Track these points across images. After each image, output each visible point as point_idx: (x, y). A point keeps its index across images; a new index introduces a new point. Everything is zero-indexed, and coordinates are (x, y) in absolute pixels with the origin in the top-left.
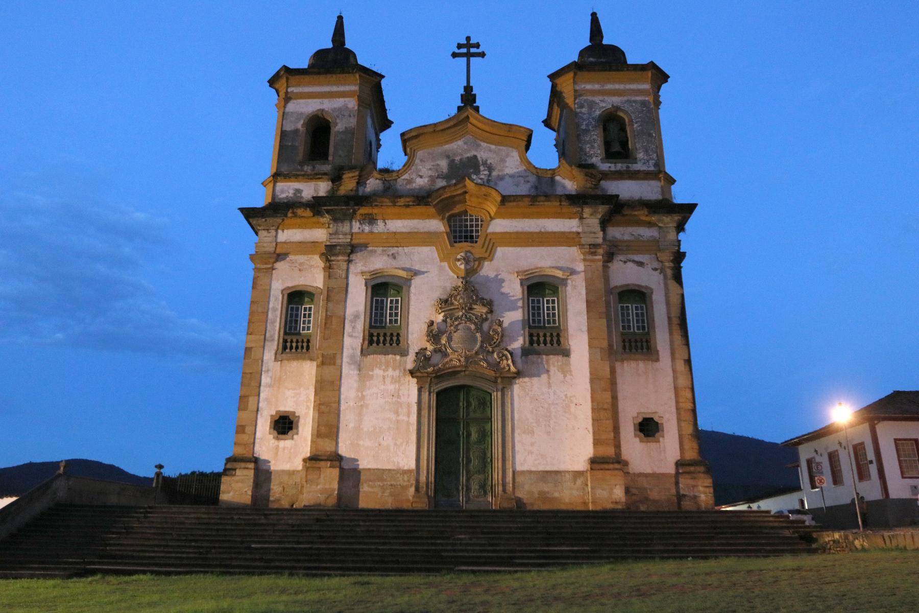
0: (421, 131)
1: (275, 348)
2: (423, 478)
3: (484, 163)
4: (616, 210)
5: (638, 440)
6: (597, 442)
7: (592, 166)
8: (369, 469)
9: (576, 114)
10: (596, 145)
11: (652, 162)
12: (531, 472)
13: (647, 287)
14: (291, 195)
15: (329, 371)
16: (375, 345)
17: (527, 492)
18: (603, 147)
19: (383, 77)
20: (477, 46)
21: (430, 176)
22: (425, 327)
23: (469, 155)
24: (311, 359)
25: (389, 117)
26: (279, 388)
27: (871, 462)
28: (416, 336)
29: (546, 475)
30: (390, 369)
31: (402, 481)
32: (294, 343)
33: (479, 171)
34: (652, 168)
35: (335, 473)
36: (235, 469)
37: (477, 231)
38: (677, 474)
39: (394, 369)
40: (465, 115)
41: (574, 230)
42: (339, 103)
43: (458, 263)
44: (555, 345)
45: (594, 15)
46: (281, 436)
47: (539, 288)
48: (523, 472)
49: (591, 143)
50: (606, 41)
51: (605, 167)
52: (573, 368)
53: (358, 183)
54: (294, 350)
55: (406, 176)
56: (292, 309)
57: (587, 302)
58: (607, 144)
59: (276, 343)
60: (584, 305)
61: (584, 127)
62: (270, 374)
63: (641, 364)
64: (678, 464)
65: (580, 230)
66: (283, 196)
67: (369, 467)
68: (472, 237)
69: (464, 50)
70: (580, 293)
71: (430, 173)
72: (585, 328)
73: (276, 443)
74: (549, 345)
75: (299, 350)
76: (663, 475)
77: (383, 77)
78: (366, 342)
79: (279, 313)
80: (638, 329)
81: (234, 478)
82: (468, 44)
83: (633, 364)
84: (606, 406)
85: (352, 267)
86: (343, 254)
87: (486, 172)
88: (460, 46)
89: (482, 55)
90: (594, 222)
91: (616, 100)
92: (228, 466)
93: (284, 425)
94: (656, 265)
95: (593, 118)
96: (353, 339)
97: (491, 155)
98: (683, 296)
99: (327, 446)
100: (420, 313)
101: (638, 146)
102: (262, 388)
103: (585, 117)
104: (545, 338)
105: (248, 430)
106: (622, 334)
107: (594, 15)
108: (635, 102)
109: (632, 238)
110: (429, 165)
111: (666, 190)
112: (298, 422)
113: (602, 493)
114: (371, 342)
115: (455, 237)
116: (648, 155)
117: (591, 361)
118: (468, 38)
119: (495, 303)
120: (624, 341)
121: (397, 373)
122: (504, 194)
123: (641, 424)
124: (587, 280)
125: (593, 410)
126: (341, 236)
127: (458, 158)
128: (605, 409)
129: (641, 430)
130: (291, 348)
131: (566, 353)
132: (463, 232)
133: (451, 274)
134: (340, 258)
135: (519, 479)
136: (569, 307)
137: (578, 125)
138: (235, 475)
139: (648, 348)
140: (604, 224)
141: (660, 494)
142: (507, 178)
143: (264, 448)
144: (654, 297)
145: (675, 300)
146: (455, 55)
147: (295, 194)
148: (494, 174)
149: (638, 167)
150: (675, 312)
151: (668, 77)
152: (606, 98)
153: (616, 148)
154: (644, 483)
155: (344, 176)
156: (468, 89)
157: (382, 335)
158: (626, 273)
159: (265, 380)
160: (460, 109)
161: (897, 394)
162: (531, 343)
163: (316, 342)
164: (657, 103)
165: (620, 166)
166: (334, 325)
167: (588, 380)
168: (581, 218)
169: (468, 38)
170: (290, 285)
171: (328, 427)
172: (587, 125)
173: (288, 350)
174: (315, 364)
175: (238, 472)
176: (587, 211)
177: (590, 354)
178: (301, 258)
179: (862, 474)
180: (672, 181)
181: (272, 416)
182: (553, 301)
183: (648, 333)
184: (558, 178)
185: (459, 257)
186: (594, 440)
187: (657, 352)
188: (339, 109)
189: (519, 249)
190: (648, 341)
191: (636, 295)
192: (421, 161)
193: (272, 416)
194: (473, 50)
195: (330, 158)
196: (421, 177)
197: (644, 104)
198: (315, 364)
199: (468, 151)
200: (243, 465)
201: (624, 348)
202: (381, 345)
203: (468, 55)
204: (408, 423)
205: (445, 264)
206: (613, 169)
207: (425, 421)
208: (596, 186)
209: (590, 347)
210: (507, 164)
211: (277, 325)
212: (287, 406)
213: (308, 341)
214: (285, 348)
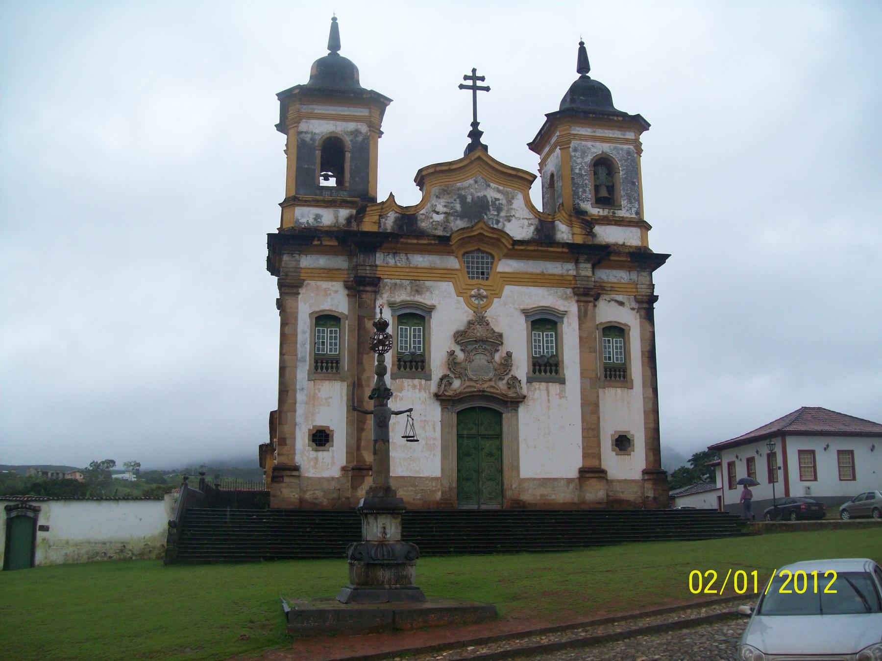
0: (438, 169)
1: (308, 368)
3: (494, 203)
4: (602, 255)
5: (614, 453)
6: (585, 456)
7: (585, 213)
8: (403, 477)
9: (571, 157)
10: (587, 189)
11: (634, 210)
12: (534, 479)
13: (626, 325)
14: (311, 221)
16: (402, 369)
17: (529, 496)
18: (593, 192)
20: (482, 79)
21: (445, 213)
23: (479, 194)
26: (314, 405)
27: (780, 468)
29: (545, 482)
30: (417, 391)
33: (489, 210)
34: (634, 216)
36: (282, 477)
37: (487, 268)
38: (644, 480)
39: (420, 390)
40: (477, 155)
41: (571, 272)
42: (351, 126)
43: (473, 299)
44: (553, 373)
45: (582, 44)
46: (319, 448)
48: (528, 479)
49: (584, 186)
50: (593, 75)
51: (595, 211)
52: (567, 394)
53: (380, 216)
54: (324, 370)
56: (319, 331)
57: (580, 338)
58: (597, 188)
59: (308, 363)
60: (577, 341)
61: (577, 171)
62: (305, 392)
63: (619, 390)
64: (645, 472)
65: (575, 273)
66: (303, 220)
67: (401, 474)
68: (483, 273)
69: (470, 83)
70: (574, 330)
71: (445, 210)
72: (578, 361)
73: (313, 454)
74: (548, 374)
75: (330, 370)
76: (634, 481)
78: (396, 367)
79: (308, 335)
80: (617, 360)
81: (284, 485)
82: (474, 77)
83: (613, 390)
84: (593, 426)
85: (378, 297)
86: (370, 284)
87: (496, 213)
88: (466, 78)
89: (487, 89)
90: (589, 266)
91: (606, 147)
92: (275, 474)
94: (634, 305)
95: (585, 163)
97: (498, 196)
98: (653, 333)
100: (440, 344)
101: (622, 193)
102: (298, 405)
103: (579, 161)
104: (547, 368)
105: (288, 441)
106: (605, 363)
107: (582, 44)
108: (622, 149)
109: (615, 280)
111: (644, 238)
112: (333, 436)
114: (399, 369)
115: (468, 273)
116: (631, 203)
117: (582, 389)
118: (474, 70)
119: (505, 336)
120: (606, 371)
121: (423, 395)
123: (617, 440)
125: (583, 429)
126: (368, 268)
128: (593, 429)
129: (617, 445)
130: (322, 368)
131: (562, 382)
133: (467, 308)
134: (368, 288)
135: (526, 485)
136: (565, 341)
137: (572, 169)
138: (283, 482)
139: (624, 377)
140: (594, 267)
141: (630, 495)
142: (513, 219)
143: (305, 458)
144: (631, 333)
145: (648, 335)
146: (462, 87)
147: (315, 219)
148: (503, 214)
149: (622, 213)
150: (648, 348)
151: (650, 125)
152: (598, 144)
153: (604, 193)
155: (368, 209)
156: (475, 124)
158: (608, 312)
159: (301, 397)
160: (470, 149)
161: (804, 410)
162: (534, 372)
163: (345, 363)
164: (639, 151)
167: (579, 405)
169: (474, 70)
170: (317, 309)
172: (580, 169)
173: (319, 370)
174: (345, 384)
175: (286, 480)
177: (581, 383)
178: (325, 285)
179: (772, 479)
180: (649, 227)
181: (309, 430)
182: (552, 335)
183: (625, 364)
184: (557, 223)
185: (473, 293)
186: (583, 453)
187: (632, 380)
188: (352, 133)
189: (525, 288)
190: (625, 371)
191: (616, 330)
192: (437, 197)
193: (309, 430)
194: (479, 83)
195: (347, 185)
196: (438, 213)
197: (629, 153)
198: (345, 384)
200: (288, 473)
201: (606, 376)
202: (408, 369)
203: (475, 88)
204: (434, 439)
205: (461, 299)
206: (601, 213)
208: (591, 234)
209: (582, 377)
210: (513, 206)
211: (308, 346)
212: (321, 421)
213: (337, 362)
214: (316, 368)
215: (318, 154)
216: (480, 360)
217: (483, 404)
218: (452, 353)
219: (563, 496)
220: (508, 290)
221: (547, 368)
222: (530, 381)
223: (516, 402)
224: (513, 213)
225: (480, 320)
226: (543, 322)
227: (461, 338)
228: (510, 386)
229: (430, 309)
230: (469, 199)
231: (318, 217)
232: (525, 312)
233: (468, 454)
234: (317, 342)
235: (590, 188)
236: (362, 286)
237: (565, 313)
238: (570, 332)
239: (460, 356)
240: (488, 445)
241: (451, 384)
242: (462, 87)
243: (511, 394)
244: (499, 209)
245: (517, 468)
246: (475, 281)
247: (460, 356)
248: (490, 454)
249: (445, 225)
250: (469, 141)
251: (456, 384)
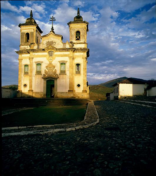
3: (54, 42)
7: (72, 42)
20: (54, 18)
28: (43, 73)
31: (42, 94)
32: (26, 73)
47: (63, 63)
63: (78, 76)
69: (52, 19)
93: (25, 85)
96: (34, 72)
99: (31, 89)
102: (22, 81)
105: (20, 86)
118: (53, 17)
132: (51, 54)
146: (50, 20)
153: (78, 38)
154: (77, 94)
158: (77, 61)
163: (29, 73)
165: (78, 42)
171: (31, 86)
194: (54, 19)
212: (25, 83)
217: (51, 79)
225: (50, 63)
227: (47, 67)
229: (42, 62)
235: (75, 37)
236: (31, 59)
238: (68, 65)
241: (45, 76)
242: (50, 20)
243: (56, 77)
244: (55, 43)
245: (56, 90)
251: (46, 75)
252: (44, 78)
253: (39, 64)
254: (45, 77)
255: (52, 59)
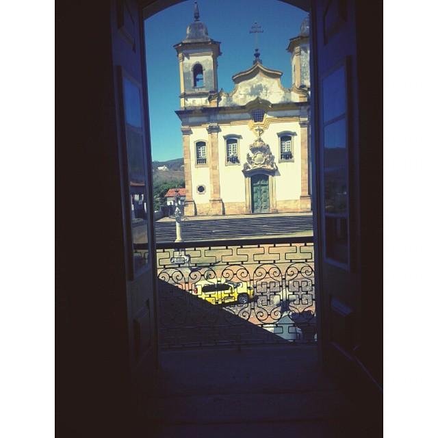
2: (248, 204)
6: (303, 190)
7: (304, 86)
15: (215, 172)
19: (220, 43)
22: (246, 157)
23: (259, 84)
24: (208, 167)
25: (221, 51)
28: (243, 160)
29: (286, 201)
31: (241, 205)
32: (201, 161)
35: (221, 204)
47: (285, 137)
55: (235, 95)
69: (253, 30)
77: (220, 43)
93: (201, 189)
104: (287, 156)
105: (190, 191)
110: (243, 89)
113: (303, 206)
122: (272, 102)
124: (302, 135)
127: (254, 86)
131: (293, 162)
146: (251, 32)
157: (234, 160)
160: (255, 62)
163: (208, 160)
166: (215, 156)
168: (300, 109)
176: (302, 107)
185: (257, 128)
194: (259, 29)
198: (208, 168)
199: (258, 82)
207: (247, 186)
215: (192, 73)
216: (259, 155)
217: (261, 173)
218: (248, 155)
219: (292, 206)
220: (272, 125)
221: (287, 156)
222: (279, 162)
223: (274, 172)
224: (272, 90)
225: (260, 140)
226: (285, 137)
228: (272, 166)
229: (240, 137)
230: (254, 86)
231: (193, 101)
232: (278, 134)
233: (256, 192)
234: (198, 154)
236: (211, 130)
237: (294, 134)
239: (252, 155)
240: (263, 188)
244: (267, 90)
246: (257, 123)
247: (252, 155)
248: (265, 192)
249: (244, 99)
250: (254, 58)
251: (250, 166)
252: (246, 173)
253: (231, 140)
254: (248, 170)
255: (261, 128)
